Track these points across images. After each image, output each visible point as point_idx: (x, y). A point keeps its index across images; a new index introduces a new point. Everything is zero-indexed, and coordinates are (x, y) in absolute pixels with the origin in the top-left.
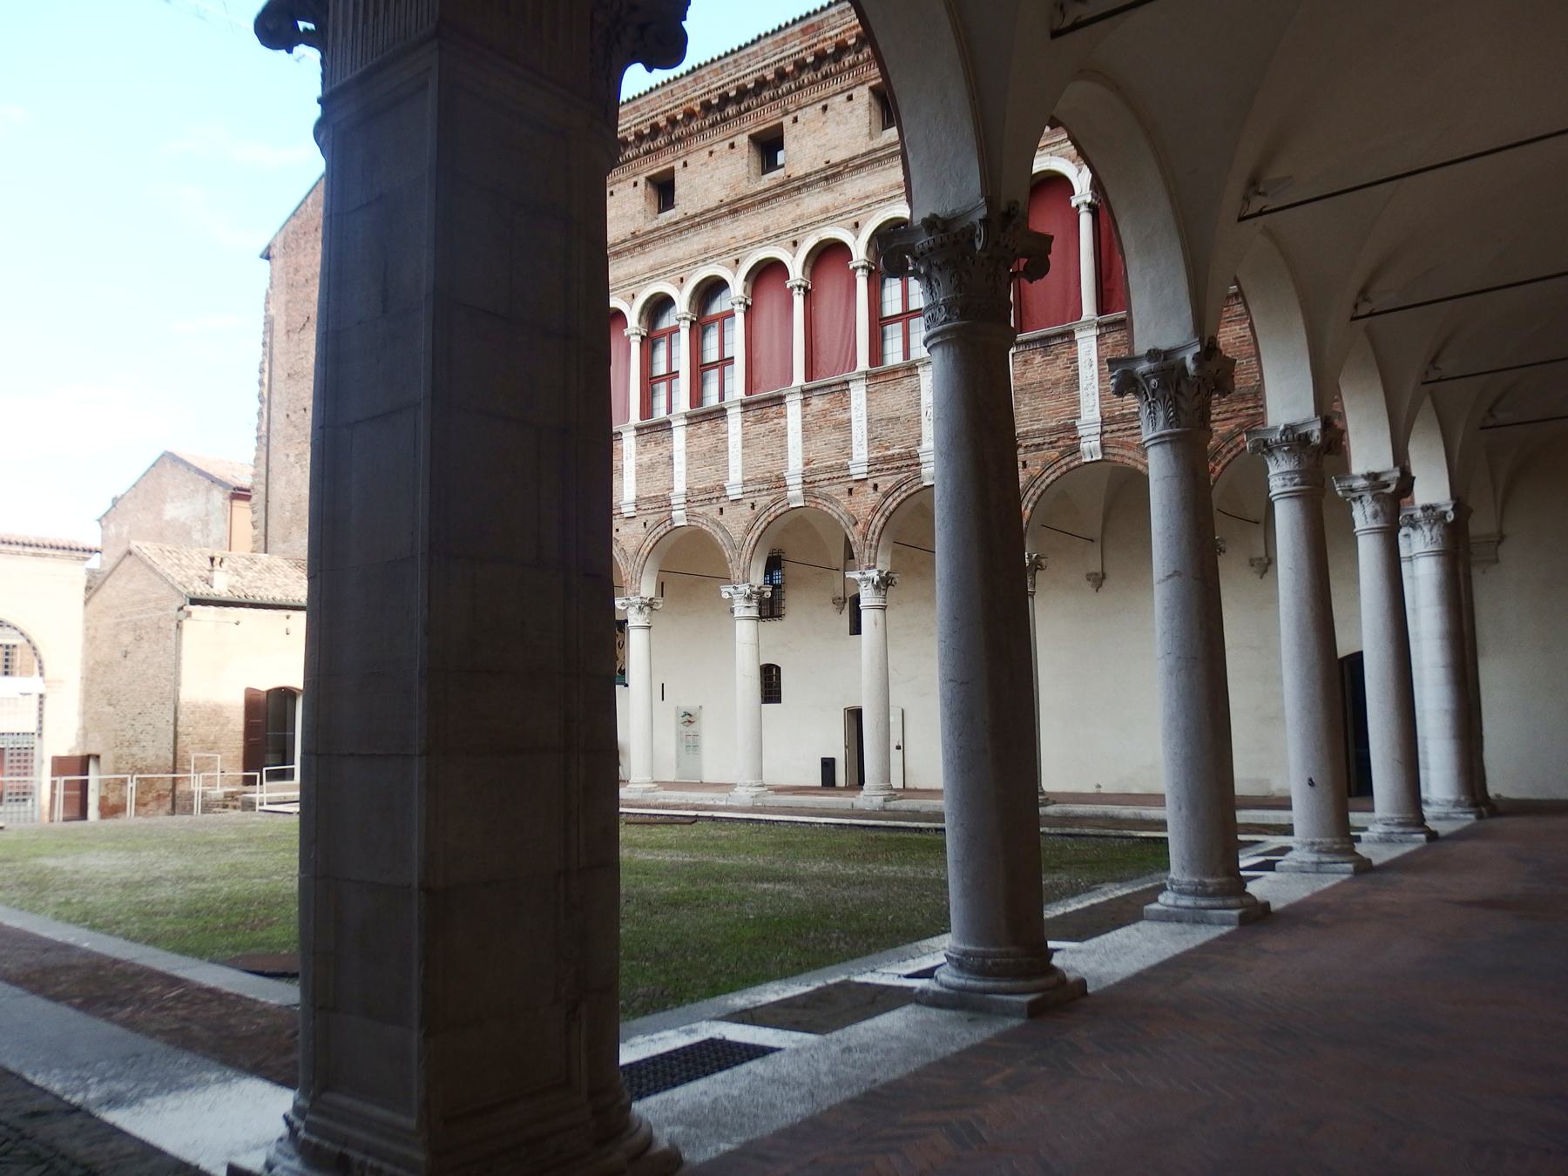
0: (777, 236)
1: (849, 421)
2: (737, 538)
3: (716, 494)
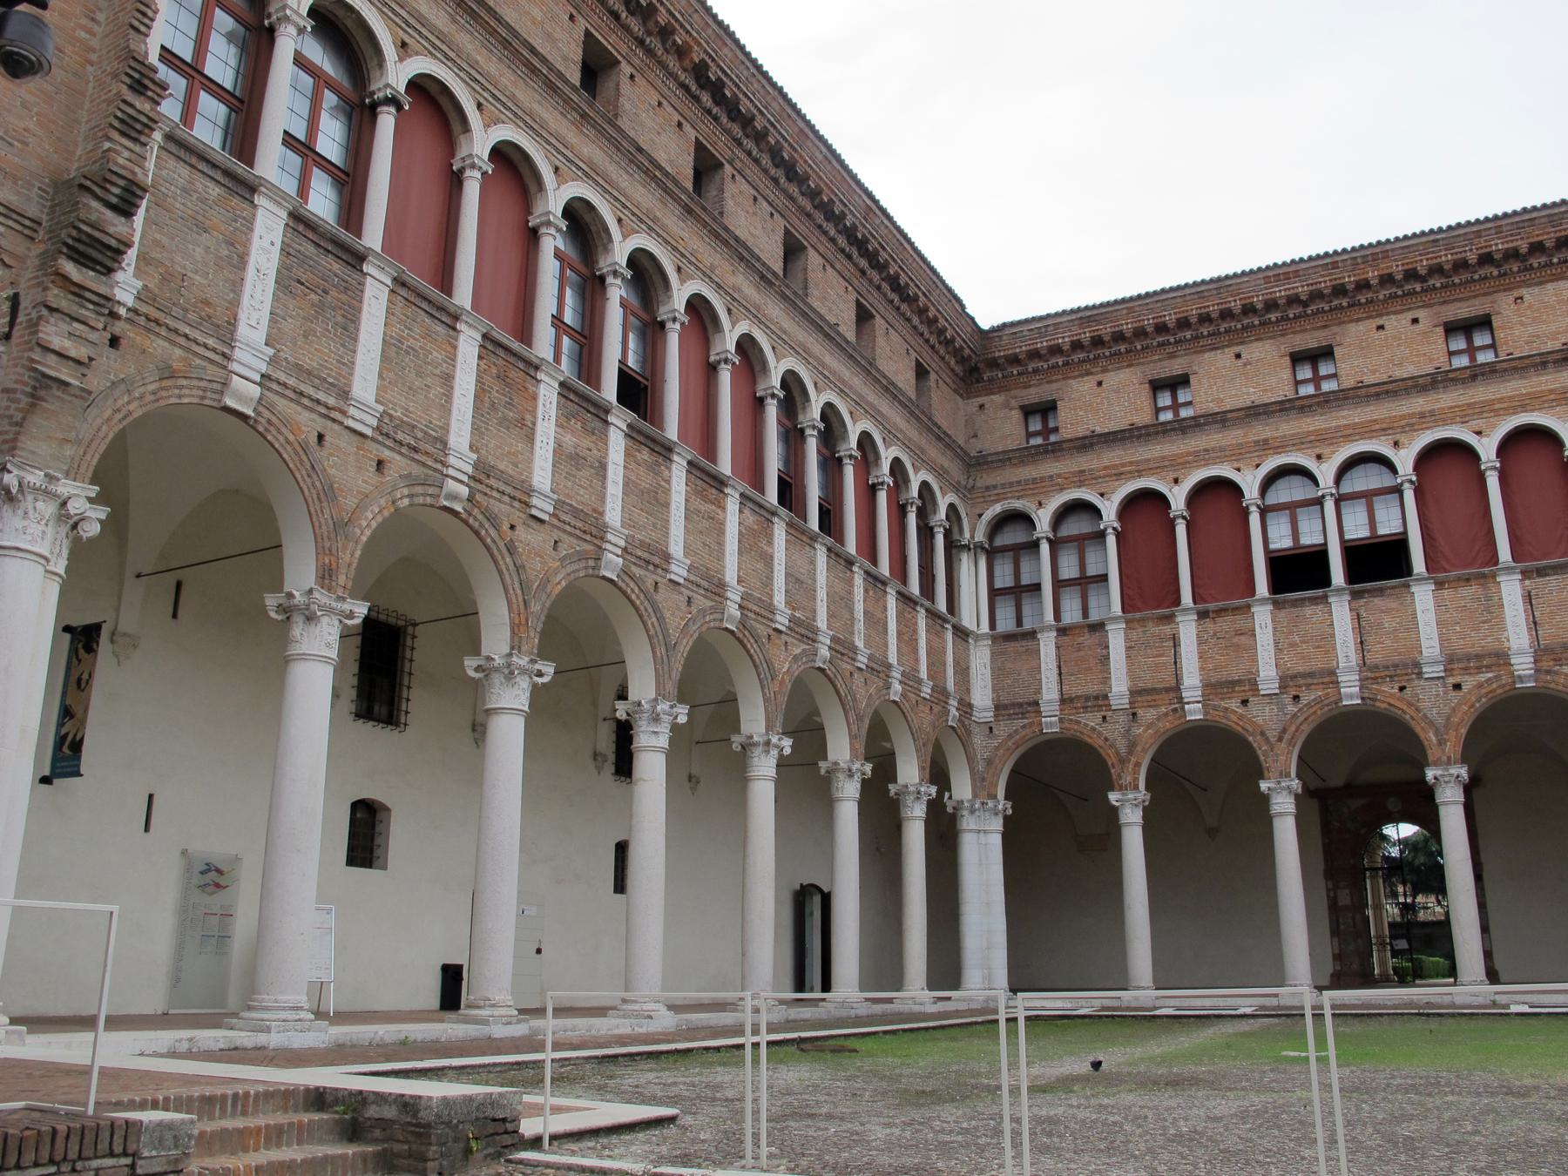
0: (720, 287)
1: (772, 557)
2: (674, 635)
3: (657, 560)
